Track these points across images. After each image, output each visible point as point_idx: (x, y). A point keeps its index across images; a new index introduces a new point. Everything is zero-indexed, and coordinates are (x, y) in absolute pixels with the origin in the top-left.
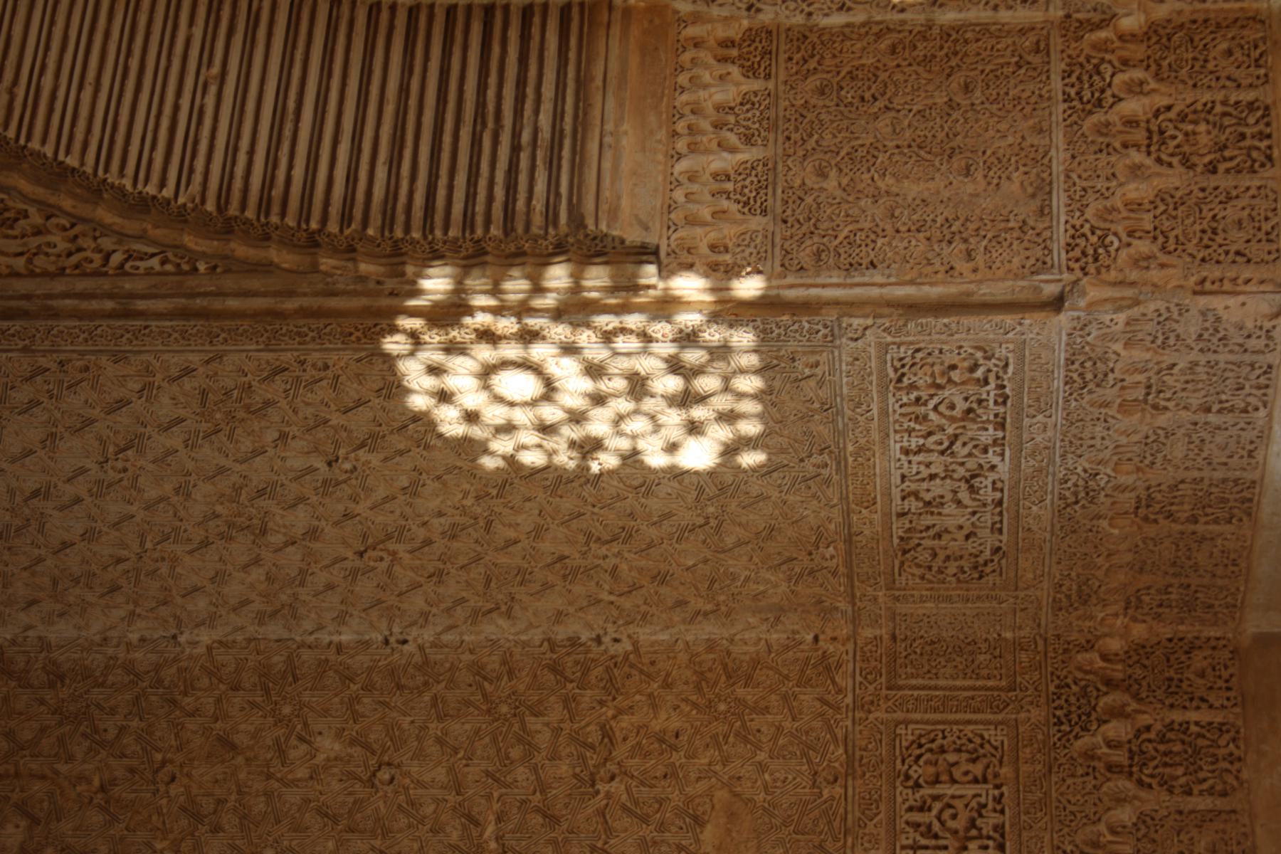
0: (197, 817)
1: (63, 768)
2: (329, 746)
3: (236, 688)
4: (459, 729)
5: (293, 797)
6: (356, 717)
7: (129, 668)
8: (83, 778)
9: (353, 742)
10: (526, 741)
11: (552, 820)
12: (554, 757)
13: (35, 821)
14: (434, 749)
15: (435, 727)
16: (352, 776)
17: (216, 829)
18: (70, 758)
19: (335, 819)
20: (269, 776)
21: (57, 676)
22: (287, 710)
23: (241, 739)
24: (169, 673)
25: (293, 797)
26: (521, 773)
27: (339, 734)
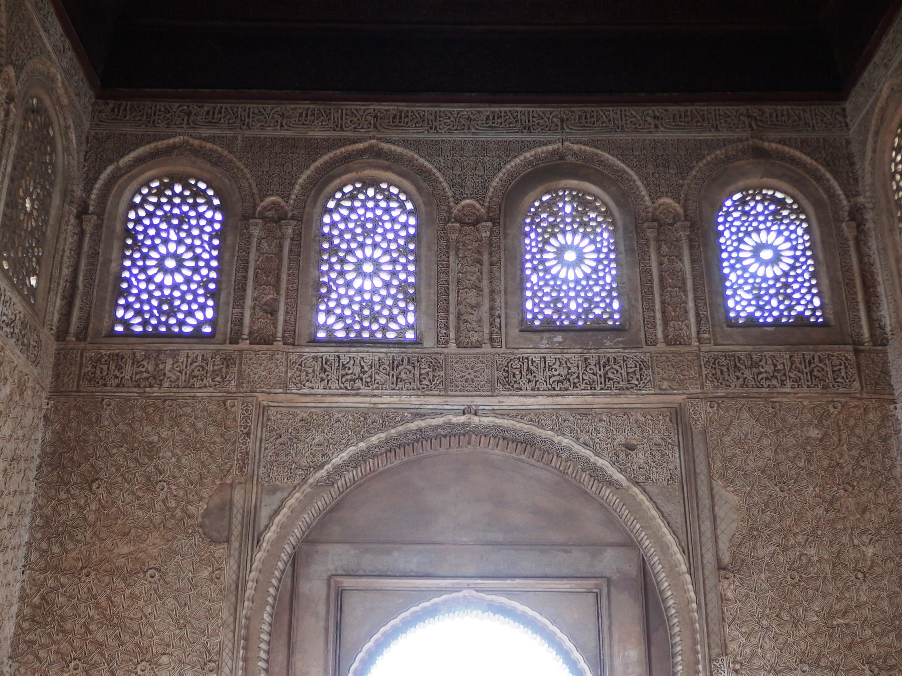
0: (831, 503)
1: (845, 447)
2: (870, 551)
3: (890, 510)
4: (885, 605)
5: (845, 539)
6: (885, 561)
7: (893, 466)
8: (841, 455)
9: (873, 561)
10: (884, 633)
11: (849, 647)
12: (878, 646)
13: (821, 440)
14: (875, 593)
15: (884, 594)
16: (857, 563)
17: (827, 511)
18: (849, 450)
19: (838, 557)
20: (852, 529)
21: (885, 439)
22: (883, 532)
23: (867, 516)
24: (892, 483)
25: (845, 539)
26: (868, 632)
27: (875, 555)
